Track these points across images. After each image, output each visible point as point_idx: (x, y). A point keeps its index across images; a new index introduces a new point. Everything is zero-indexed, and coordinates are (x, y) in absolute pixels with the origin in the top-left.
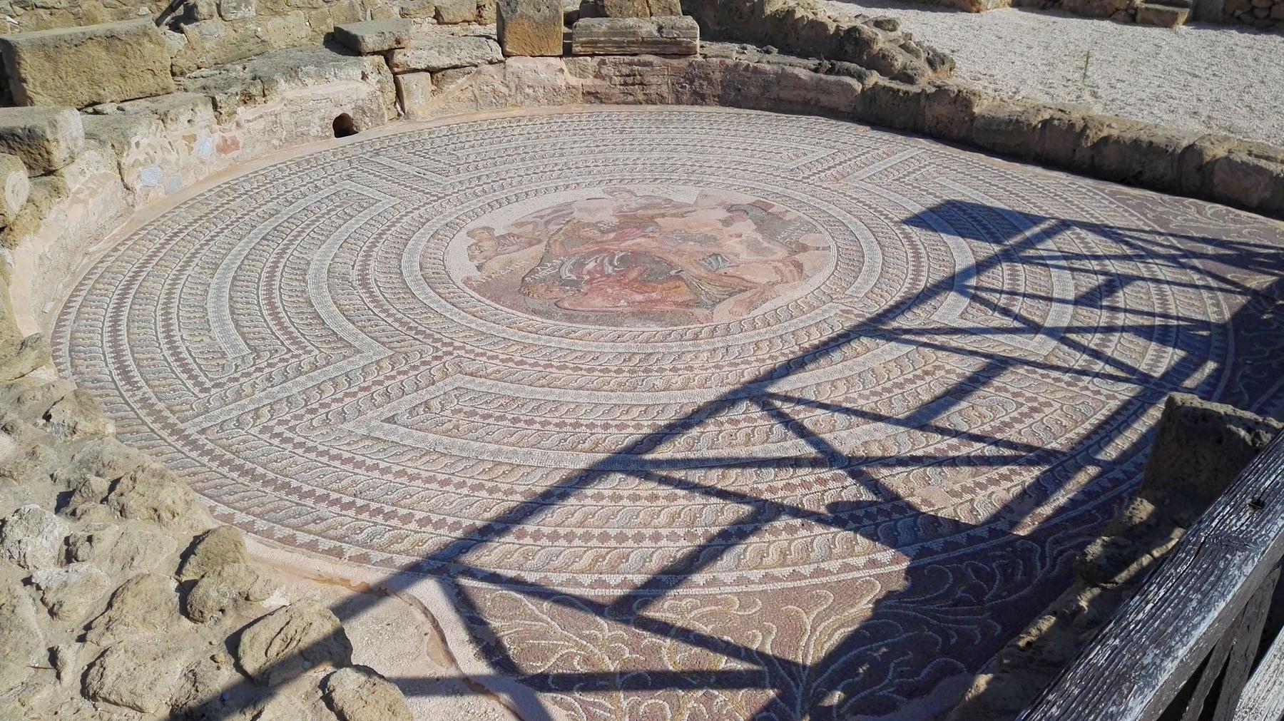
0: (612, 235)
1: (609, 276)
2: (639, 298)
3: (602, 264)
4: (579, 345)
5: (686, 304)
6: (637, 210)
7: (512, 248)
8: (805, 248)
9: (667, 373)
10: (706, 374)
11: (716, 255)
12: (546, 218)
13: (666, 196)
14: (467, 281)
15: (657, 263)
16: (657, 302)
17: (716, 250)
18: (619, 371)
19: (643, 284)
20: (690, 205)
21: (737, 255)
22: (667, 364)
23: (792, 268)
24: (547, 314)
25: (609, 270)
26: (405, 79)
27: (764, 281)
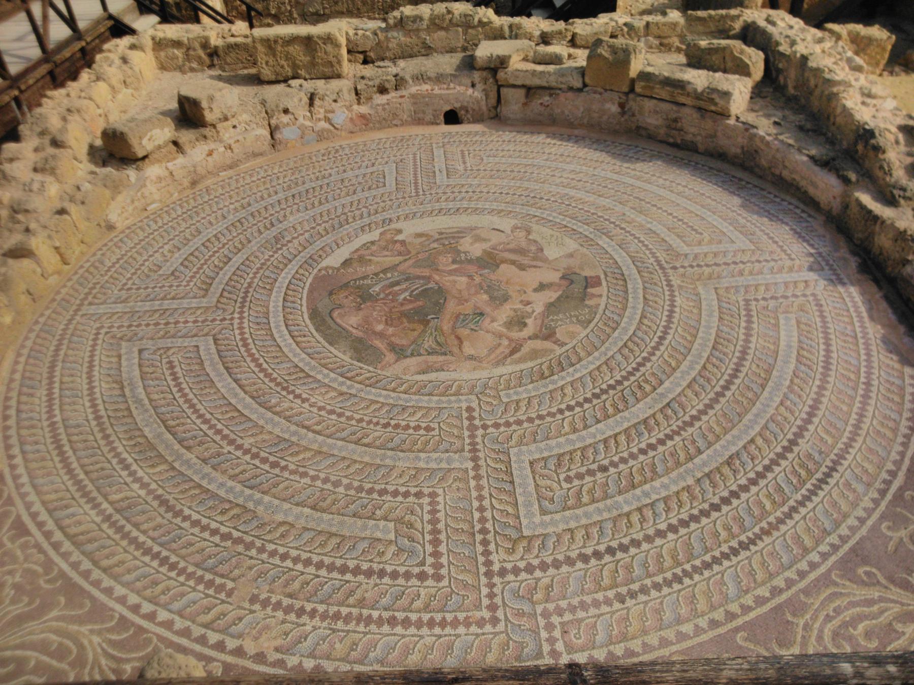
26: (504, 91)
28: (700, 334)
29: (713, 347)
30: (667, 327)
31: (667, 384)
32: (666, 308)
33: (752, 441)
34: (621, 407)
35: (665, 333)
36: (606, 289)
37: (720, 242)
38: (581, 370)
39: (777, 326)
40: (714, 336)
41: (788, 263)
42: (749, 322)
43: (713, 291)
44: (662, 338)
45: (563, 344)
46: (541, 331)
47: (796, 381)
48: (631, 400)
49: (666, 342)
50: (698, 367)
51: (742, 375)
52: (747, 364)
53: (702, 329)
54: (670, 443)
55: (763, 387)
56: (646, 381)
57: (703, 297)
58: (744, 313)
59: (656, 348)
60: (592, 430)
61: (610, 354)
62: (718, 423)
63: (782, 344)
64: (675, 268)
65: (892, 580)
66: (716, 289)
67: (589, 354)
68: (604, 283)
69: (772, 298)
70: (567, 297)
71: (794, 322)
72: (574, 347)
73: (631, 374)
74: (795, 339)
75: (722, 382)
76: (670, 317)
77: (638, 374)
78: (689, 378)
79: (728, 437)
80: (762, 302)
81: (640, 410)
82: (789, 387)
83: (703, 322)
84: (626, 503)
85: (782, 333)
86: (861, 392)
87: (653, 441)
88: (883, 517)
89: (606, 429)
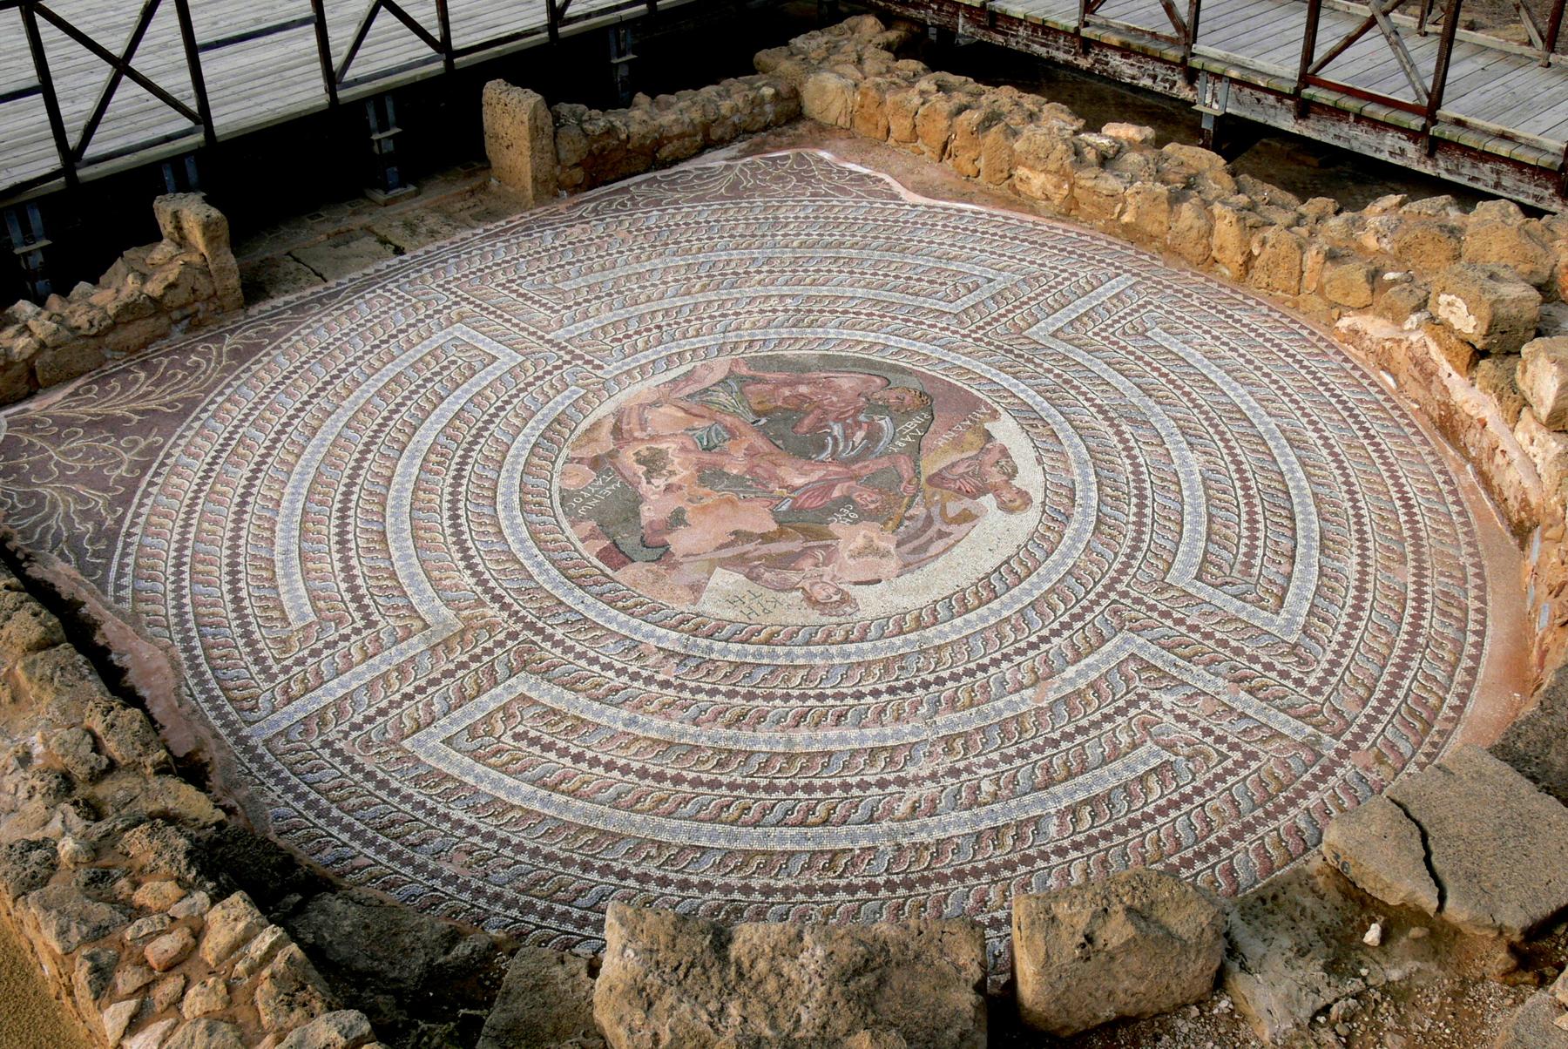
0: (836, 493)
1: (837, 420)
2: (803, 389)
3: (846, 438)
4: (858, 335)
5: (756, 380)
6: (803, 554)
7: (961, 469)
8: (595, 463)
10: (748, 308)
11: (708, 449)
12: (932, 532)
13: (756, 588)
14: (994, 415)
15: (781, 437)
16: (786, 384)
17: (706, 457)
18: (821, 311)
19: (798, 407)
20: (725, 563)
21: (684, 449)
22: (781, 316)
23: (625, 427)
24: (894, 368)
25: (837, 430)
27: (666, 409)
28: (410, 542)
29: (384, 533)
30: (458, 533)
31: (415, 471)
33: (298, 456)
34: (450, 431)
35: (455, 526)
36: (586, 554)
37: (471, 731)
38: (520, 447)
39: (314, 599)
40: (392, 550)
41: (332, 733)
42: (353, 589)
43: (429, 619)
44: (455, 517)
45: (570, 460)
46: (613, 464)
47: (267, 534)
48: (443, 440)
49: (446, 514)
50: (390, 502)
51: (335, 514)
52: (334, 530)
53: (412, 551)
54: (380, 421)
55: (305, 512)
56: (438, 463)
57: (438, 602)
58: (366, 601)
59: (454, 502)
60: (462, 402)
61: (504, 474)
62: (341, 458)
63: (298, 576)
64: (513, 636)
65: (154, 411)
66: (426, 626)
67: (527, 463)
68: (596, 562)
69: (336, 643)
70: (627, 520)
71: (291, 616)
72: (553, 463)
73: (463, 463)
74: (282, 590)
75: (355, 497)
76: (464, 550)
77: (454, 467)
78: (394, 487)
79: (324, 450)
80: (348, 631)
81: (427, 435)
82: (275, 523)
83: (415, 560)
84: (391, 370)
85: (303, 592)
86: (188, 552)
87: (396, 417)
88: (162, 447)
89: (450, 406)
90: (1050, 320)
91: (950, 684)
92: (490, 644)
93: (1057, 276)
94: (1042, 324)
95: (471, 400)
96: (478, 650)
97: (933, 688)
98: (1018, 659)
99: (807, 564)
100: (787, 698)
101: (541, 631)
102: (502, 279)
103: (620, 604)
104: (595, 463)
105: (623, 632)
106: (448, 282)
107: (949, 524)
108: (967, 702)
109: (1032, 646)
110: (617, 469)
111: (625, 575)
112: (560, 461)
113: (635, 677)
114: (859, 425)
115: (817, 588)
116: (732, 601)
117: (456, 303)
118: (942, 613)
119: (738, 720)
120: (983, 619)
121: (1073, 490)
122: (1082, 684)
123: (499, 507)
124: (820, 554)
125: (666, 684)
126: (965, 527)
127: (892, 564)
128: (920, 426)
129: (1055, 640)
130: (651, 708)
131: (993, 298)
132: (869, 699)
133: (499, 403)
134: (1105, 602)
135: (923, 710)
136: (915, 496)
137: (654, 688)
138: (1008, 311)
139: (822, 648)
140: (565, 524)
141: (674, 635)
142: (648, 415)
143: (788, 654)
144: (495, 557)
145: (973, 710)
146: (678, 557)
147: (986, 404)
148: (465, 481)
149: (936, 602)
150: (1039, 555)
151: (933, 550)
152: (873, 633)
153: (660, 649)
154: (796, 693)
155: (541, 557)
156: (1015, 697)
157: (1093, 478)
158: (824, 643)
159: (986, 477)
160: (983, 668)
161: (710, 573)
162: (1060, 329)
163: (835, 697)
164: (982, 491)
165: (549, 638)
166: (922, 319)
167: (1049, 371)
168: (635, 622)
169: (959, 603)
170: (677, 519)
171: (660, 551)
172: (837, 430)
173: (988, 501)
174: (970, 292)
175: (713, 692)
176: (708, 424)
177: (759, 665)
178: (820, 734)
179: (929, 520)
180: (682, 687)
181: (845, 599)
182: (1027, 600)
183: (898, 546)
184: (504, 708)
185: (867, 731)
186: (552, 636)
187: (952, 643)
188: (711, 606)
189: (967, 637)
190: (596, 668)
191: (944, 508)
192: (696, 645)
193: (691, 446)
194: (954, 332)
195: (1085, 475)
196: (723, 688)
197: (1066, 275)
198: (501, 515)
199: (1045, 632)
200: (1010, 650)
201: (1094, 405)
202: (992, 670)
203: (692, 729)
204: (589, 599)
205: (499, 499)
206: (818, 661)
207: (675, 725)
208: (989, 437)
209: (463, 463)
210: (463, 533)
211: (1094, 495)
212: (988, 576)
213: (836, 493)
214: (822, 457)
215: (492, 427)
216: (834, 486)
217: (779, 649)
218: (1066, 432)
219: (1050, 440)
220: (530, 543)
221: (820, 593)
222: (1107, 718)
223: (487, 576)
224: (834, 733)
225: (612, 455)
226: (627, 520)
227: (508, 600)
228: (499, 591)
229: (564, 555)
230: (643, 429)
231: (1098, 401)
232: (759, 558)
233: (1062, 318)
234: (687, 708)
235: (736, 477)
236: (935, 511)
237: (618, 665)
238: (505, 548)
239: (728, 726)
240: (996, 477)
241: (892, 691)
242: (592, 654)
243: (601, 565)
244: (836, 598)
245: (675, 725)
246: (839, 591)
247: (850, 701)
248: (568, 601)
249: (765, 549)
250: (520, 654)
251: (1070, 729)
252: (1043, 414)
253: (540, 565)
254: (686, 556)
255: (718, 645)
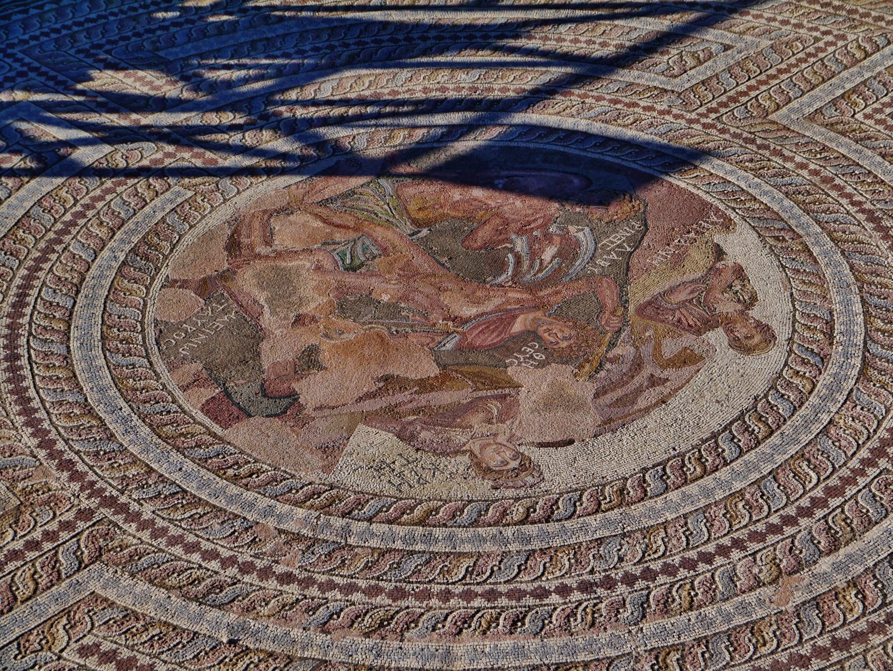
0: (518, 327)
1: (520, 232)
6: (472, 406)
7: (682, 296)
8: (204, 288)
9: (451, 86)
11: (352, 269)
12: (640, 379)
14: (727, 225)
17: (351, 279)
21: (318, 268)
23: (245, 241)
25: (520, 245)
27: (298, 218)
32: (41, 414)
64: (85, 514)
68: (200, 417)
73: (26, 287)
76: (24, 401)
90: (805, 98)
91: (662, 579)
92: (54, 526)
93: (817, 40)
94: (795, 104)
95: (39, 203)
96: (37, 534)
97: (640, 584)
98: (753, 546)
99: (475, 419)
100: (446, 596)
101: (123, 509)
102: (83, 41)
103: (230, 472)
104: (204, 288)
105: (233, 509)
106: (12, 46)
107: (663, 367)
108: (686, 605)
109: (774, 529)
110: (232, 295)
111: (240, 435)
112: (157, 284)
113: (246, 568)
114: (548, 237)
115: (489, 451)
116: (379, 468)
117: (22, 74)
118: (653, 485)
119: (381, 625)
120: (707, 492)
121: (830, 324)
122: (840, 581)
123: (74, 344)
124: (495, 408)
125: (286, 578)
126: (686, 371)
127: (590, 420)
128: (629, 240)
129: (804, 522)
130: (265, 611)
131: (729, 69)
132: (555, 598)
133: (78, 208)
134: (872, 472)
135: (625, 615)
136: (619, 331)
137: (272, 584)
138: (751, 88)
139: (494, 530)
140: (160, 367)
141: (301, 512)
142: (276, 224)
143: (450, 538)
144: (63, 409)
145: (693, 614)
146: (309, 411)
147: (718, 210)
148: (28, 310)
149: (645, 470)
150: (783, 408)
151: (641, 403)
152: (562, 509)
153: (280, 532)
154: (459, 589)
155: (126, 410)
156: (751, 598)
157: (858, 307)
158: (496, 524)
159: (716, 308)
160: (707, 558)
161: (351, 430)
162: (819, 111)
163: (510, 595)
164: (709, 324)
165: (134, 517)
166: (635, 99)
167: (802, 166)
168: (250, 495)
169: (675, 471)
170: (309, 360)
171: (285, 402)
172: (520, 245)
173: (717, 337)
174: (700, 62)
175: (351, 588)
176: (352, 235)
177: (412, 553)
178: (488, 645)
179: (638, 365)
180: (308, 582)
181: (526, 465)
182: (767, 469)
183: (597, 395)
184: (67, 612)
185: (551, 642)
186: (138, 514)
187: (665, 525)
188: (350, 475)
189: (685, 516)
190: (196, 557)
191: (658, 347)
192: (328, 525)
193: (327, 264)
194: (676, 117)
195: (848, 303)
196: (362, 583)
197: (830, 38)
198: (76, 355)
199: (791, 511)
200: (742, 534)
201: (863, 211)
202: (719, 560)
203: (320, 638)
204: (189, 465)
205: (74, 333)
206: (488, 547)
207: (296, 633)
208: (719, 253)
209: (26, 287)
210: (24, 378)
211: (860, 329)
212: (714, 436)
213: (518, 327)
214: (501, 279)
215: (67, 238)
216: (514, 317)
217: (438, 532)
218: (821, 247)
219: (803, 257)
220: (113, 392)
221: (493, 458)
222: (874, 628)
223: (53, 435)
224: (507, 643)
225: (225, 276)
226: (244, 362)
227: (80, 467)
228: (69, 455)
229: (158, 407)
230: (268, 243)
231: (868, 206)
232: (414, 412)
233: (821, 96)
234: (315, 610)
235: (388, 305)
236: (647, 350)
237: (225, 553)
238: (81, 399)
239: (367, 635)
240: (727, 307)
241: (585, 587)
242: (191, 538)
243: (207, 421)
244: (514, 464)
245: (296, 633)
246: (517, 455)
247: (530, 601)
248: (162, 469)
249: (423, 400)
250: (92, 538)
251: (824, 641)
252: (792, 223)
253: (125, 420)
254: (321, 408)
255: (358, 527)
